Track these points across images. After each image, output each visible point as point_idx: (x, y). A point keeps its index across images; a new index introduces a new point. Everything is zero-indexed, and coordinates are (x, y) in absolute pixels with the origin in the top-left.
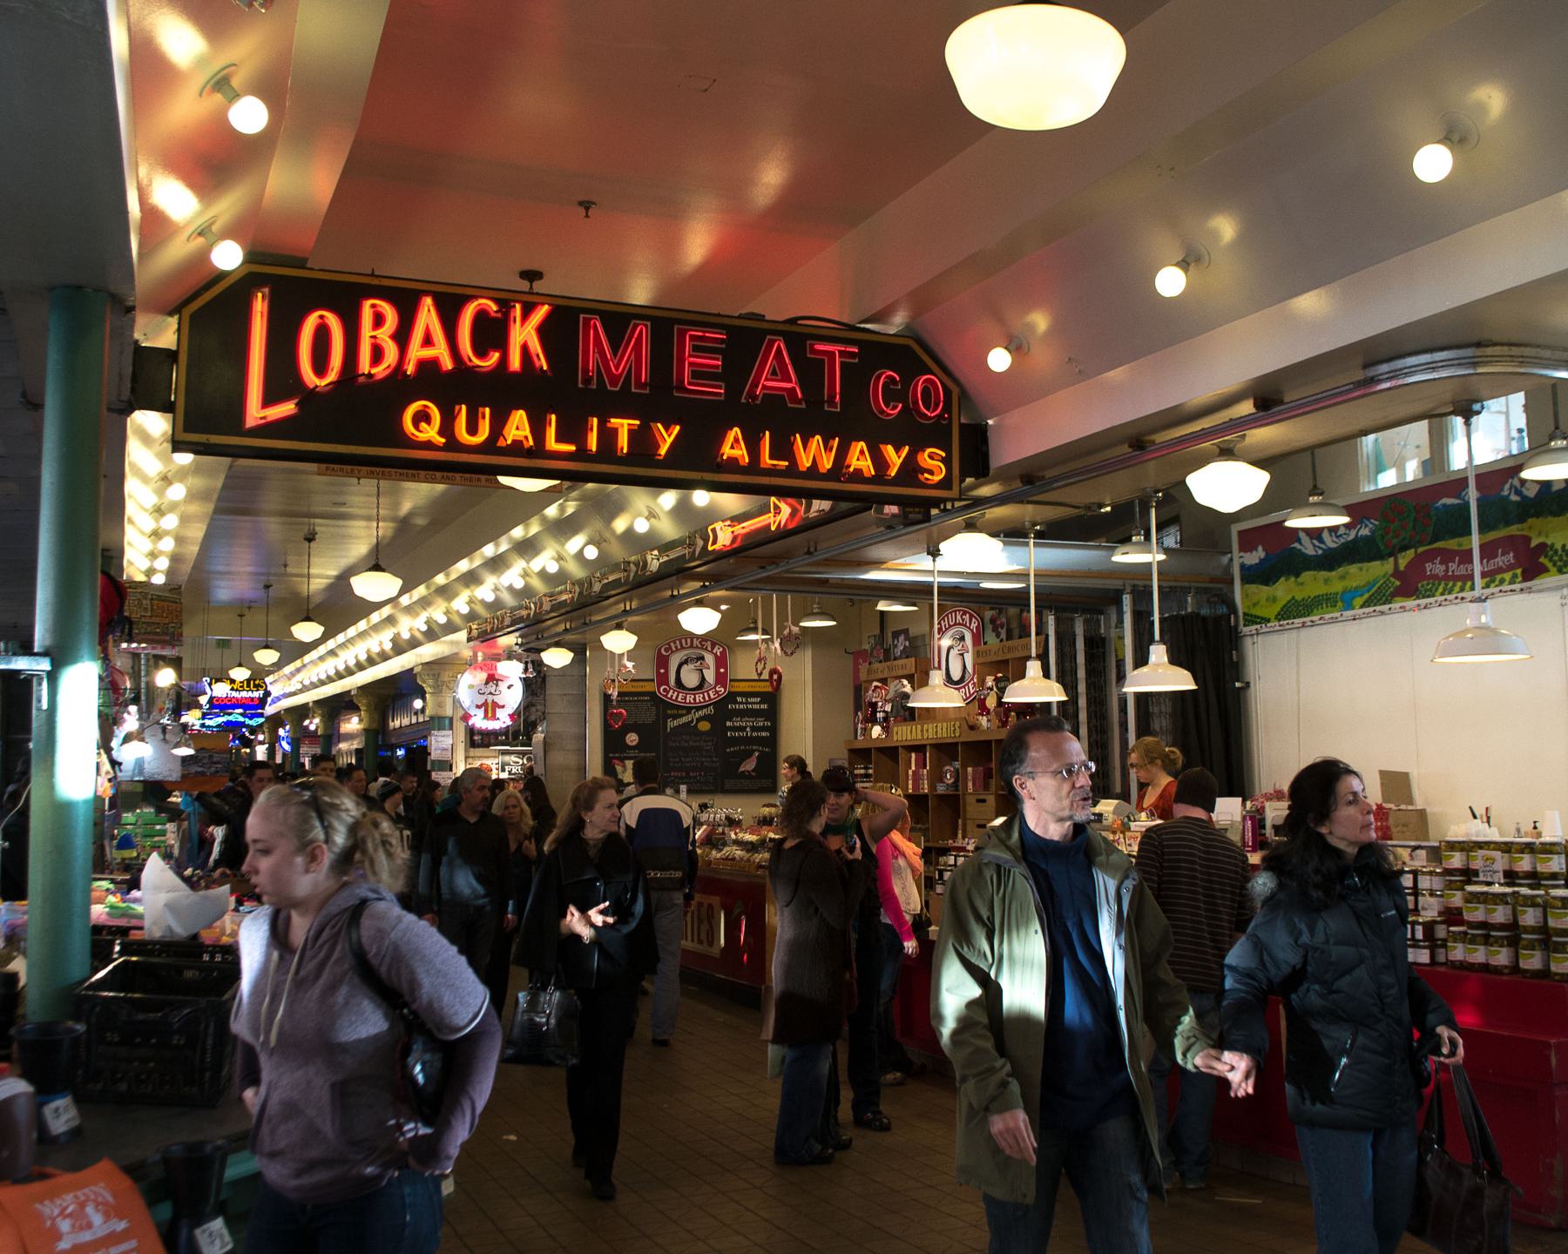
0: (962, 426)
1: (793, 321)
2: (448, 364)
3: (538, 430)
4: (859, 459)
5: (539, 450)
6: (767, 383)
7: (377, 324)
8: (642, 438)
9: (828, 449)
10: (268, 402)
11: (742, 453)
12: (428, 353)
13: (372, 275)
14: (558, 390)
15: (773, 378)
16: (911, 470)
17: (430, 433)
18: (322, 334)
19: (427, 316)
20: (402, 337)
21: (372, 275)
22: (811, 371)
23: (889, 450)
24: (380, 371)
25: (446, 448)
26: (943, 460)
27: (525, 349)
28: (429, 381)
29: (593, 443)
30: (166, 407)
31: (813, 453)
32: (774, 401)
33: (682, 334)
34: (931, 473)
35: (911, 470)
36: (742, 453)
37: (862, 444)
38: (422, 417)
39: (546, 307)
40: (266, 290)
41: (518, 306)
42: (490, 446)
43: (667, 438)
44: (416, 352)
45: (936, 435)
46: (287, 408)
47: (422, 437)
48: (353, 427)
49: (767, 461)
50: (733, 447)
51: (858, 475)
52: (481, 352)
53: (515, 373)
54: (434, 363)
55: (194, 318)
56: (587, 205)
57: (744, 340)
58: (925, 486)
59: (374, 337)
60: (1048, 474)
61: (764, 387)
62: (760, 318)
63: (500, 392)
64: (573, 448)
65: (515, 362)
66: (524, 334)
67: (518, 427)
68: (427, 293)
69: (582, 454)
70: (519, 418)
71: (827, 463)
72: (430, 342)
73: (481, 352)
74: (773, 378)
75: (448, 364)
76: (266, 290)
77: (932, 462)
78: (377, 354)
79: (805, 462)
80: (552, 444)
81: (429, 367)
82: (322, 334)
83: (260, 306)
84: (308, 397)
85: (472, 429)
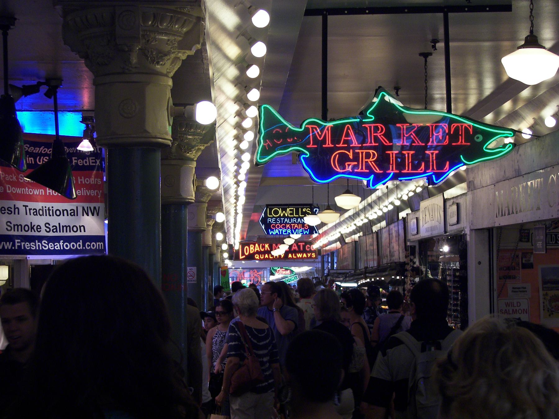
10: (242, 256)
17: (258, 258)
19: (257, 245)
20: (254, 248)
28: (258, 252)
31: (299, 255)
44: (256, 249)
66: (267, 246)
72: (257, 248)
81: (257, 251)
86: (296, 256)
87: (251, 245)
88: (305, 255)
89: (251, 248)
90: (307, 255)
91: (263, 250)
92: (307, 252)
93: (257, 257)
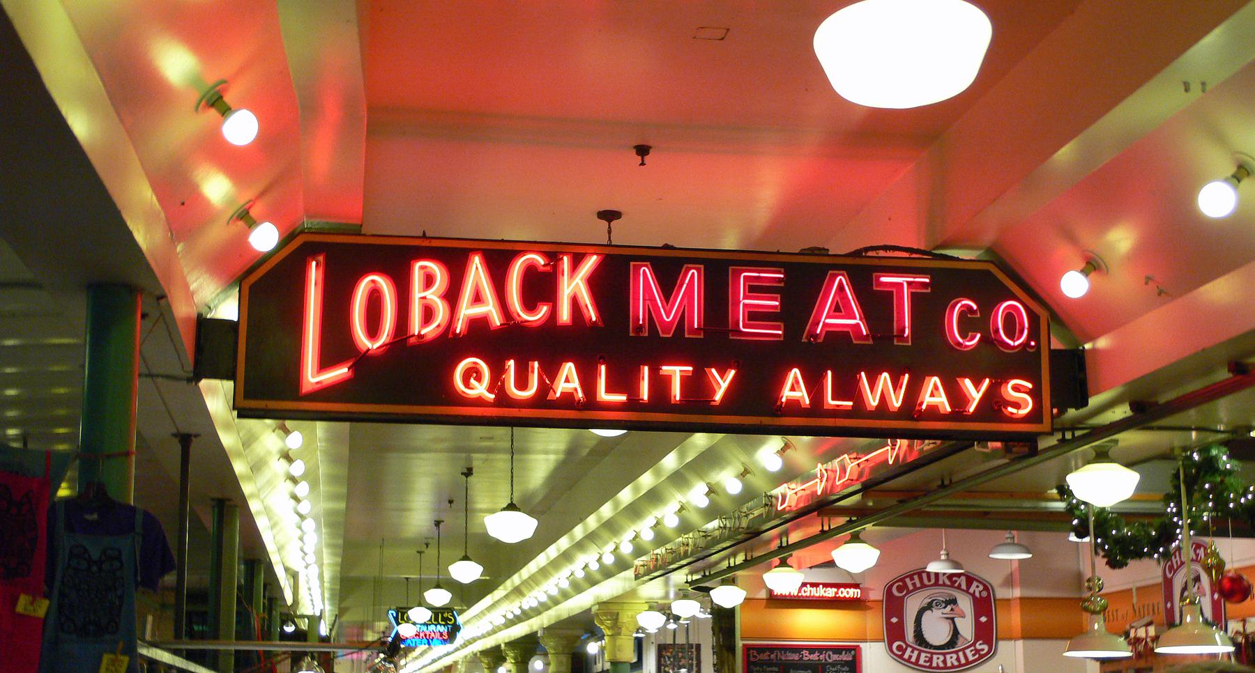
0: (1054, 354)
1: (857, 254)
2: (497, 320)
3: (588, 382)
4: (934, 395)
5: (591, 402)
6: (827, 320)
7: (427, 282)
8: (697, 386)
9: (896, 385)
10: (325, 363)
11: (802, 395)
12: (478, 310)
13: (424, 236)
14: (610, 340)
15: (839, 314)
16: (993, 405)
17: (480, 389)
18: (374, 300)
19: (477, 272)
20: (452, 296)
21: (424, 236)
22: (877, 305)
23: (968, 384)
24: (430, 331)
26: (1030, 392)
27: (575, 302)
29: (645, 393)
30: (229, 375)
31: (882, 391)
32: (838, 338)
33: (737, 275)
34: (1017, 405)
35: (993, 405)
36: (802, 395)
37: (936, 379)
39: (595, 258)
40: (321, 258)
41: (565, 258)
42: (541, 399)
43: (722, 383)
44: (467, 310)
45: (1023, 363)
47: (472, 393)
48: (401, 387)
49: (830, 402)
50: (794, 389)
51: (933, 413)
52: (530, 306)
53: (564, 328)
55: (253, 288)
56: (642, 151)
57: (802, 278)
58: (1012, 419)
59: (424, 298)
60: (1163, 399)
61: (825, 325)
62: (822, 252)
63: (547, 345)
64: (622, 398)
65: (565, 315)
66: (574, 286)
67: (568, 380)
68: (475, 251)
69: (633, 404)
70: (569, 368)
71: (896, 402)
72: (480, 302)
73: (530, 306)
74: (839, 314)
75: (497, 320)
77: (1019, 396)
78: (428, 314)
79: (873, 401)
80: (603, 396)
81: (479, 324)
82: (374, 300)
83: (314, 274)
84: (362, 361)
85: (522, 383)
87: (419, 268)
88: (934, 395)
90: (956, 397)
92: (953, 368)
93: (473, 381)
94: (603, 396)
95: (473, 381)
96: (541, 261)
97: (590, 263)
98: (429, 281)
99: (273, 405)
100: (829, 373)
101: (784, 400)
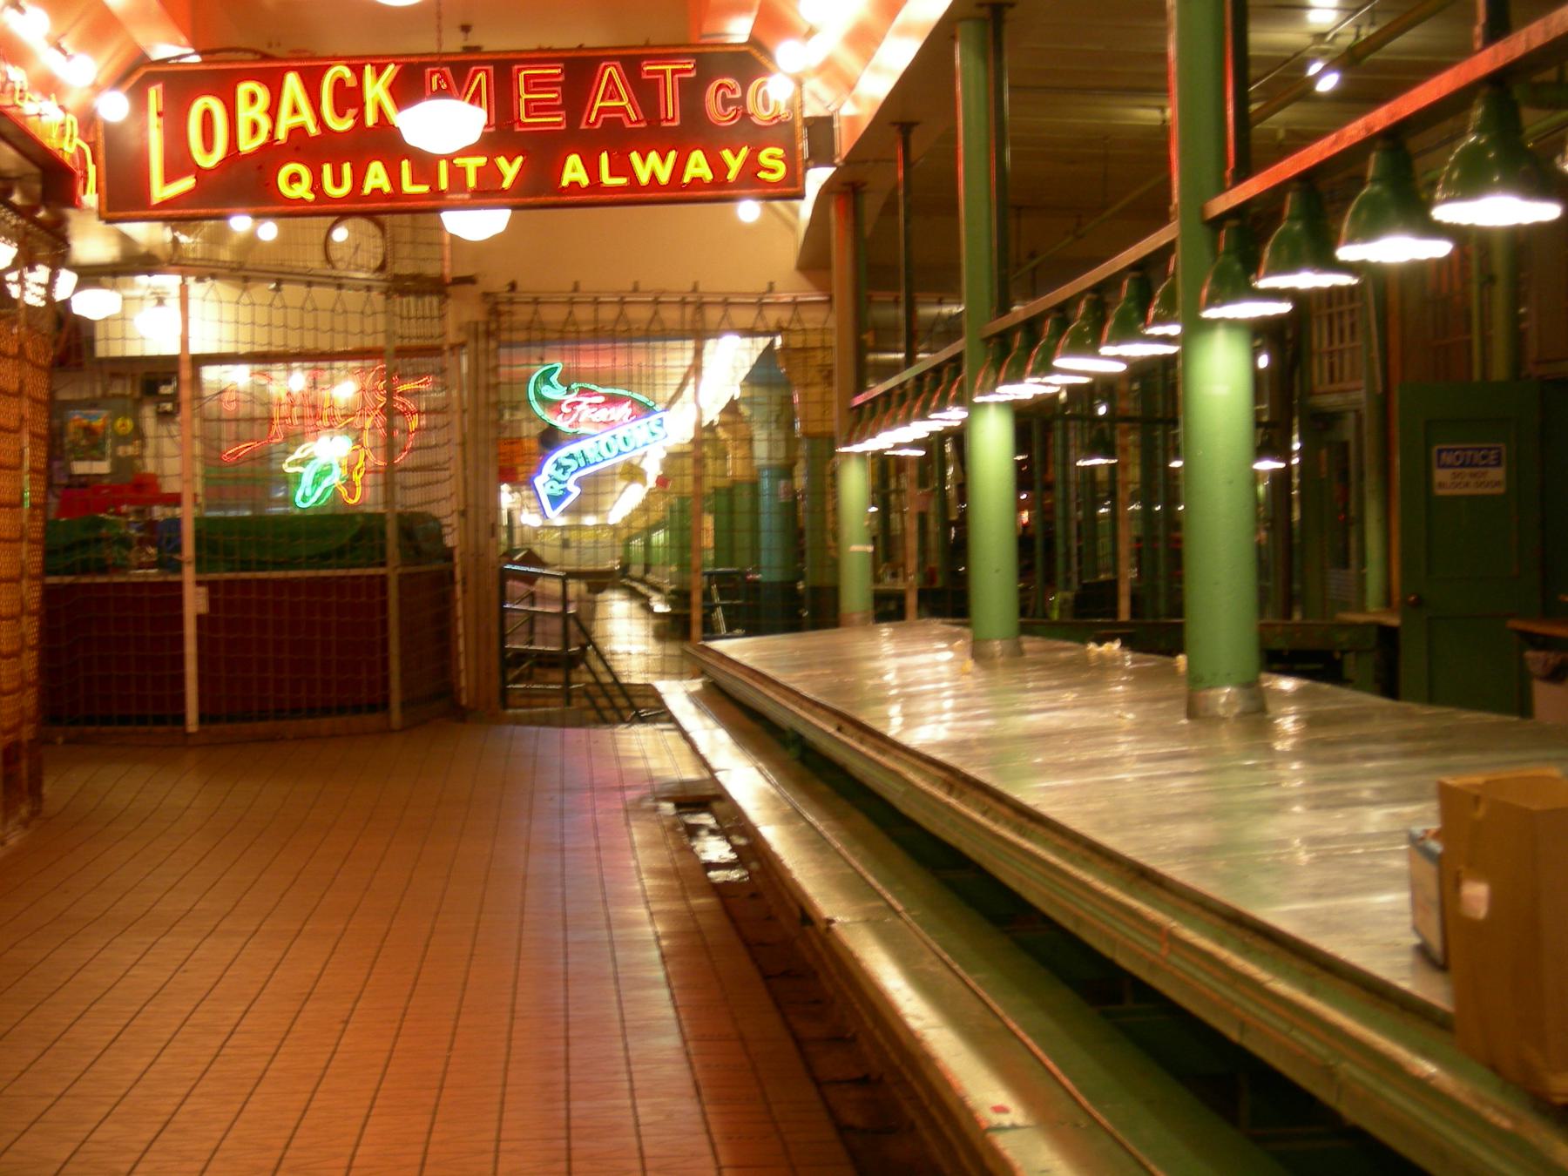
2: (313, 130)
3: (395, 178)
7: (251, 101)
9: (663, 159)
10: (169, 178)
12: (296, 121)
17: (302, 191)
18: (207, 116)
19: (293, 85)
20: (273, 112)
22: (646, 92)
23: (727, 154)
25: (316, 201)
28: (301, 146)
29: (444, 184)
31: (652, 167)
34: (773, 171)
38: (295, 178)
40: (159, 86)
43: (510, 170)
44: (286, 122)
46: (188, 183)
54: (301, 129)
57: (579, 71)
64: (424, 189)
65: (371, 119)
71: (664, 176)
73: (340, 113)
75: (313, 130)
76: (159, 86)
78: (255, 128)
79: (644, 178)
81: (298, 132)
82: (207, 116)
85: (338, 183)
86: (629, 172)
87: (244, 89)
89: (245, 114)
90: (718, 167)
91: (342, 125)
93: (295, 182)
94: (408, 187)
95: (295, 182)
96: (347, 73)
97: (391, 71)
98: (253, 98)
99: (133, 213)
100: (604, 157)
101: (565, 183)
